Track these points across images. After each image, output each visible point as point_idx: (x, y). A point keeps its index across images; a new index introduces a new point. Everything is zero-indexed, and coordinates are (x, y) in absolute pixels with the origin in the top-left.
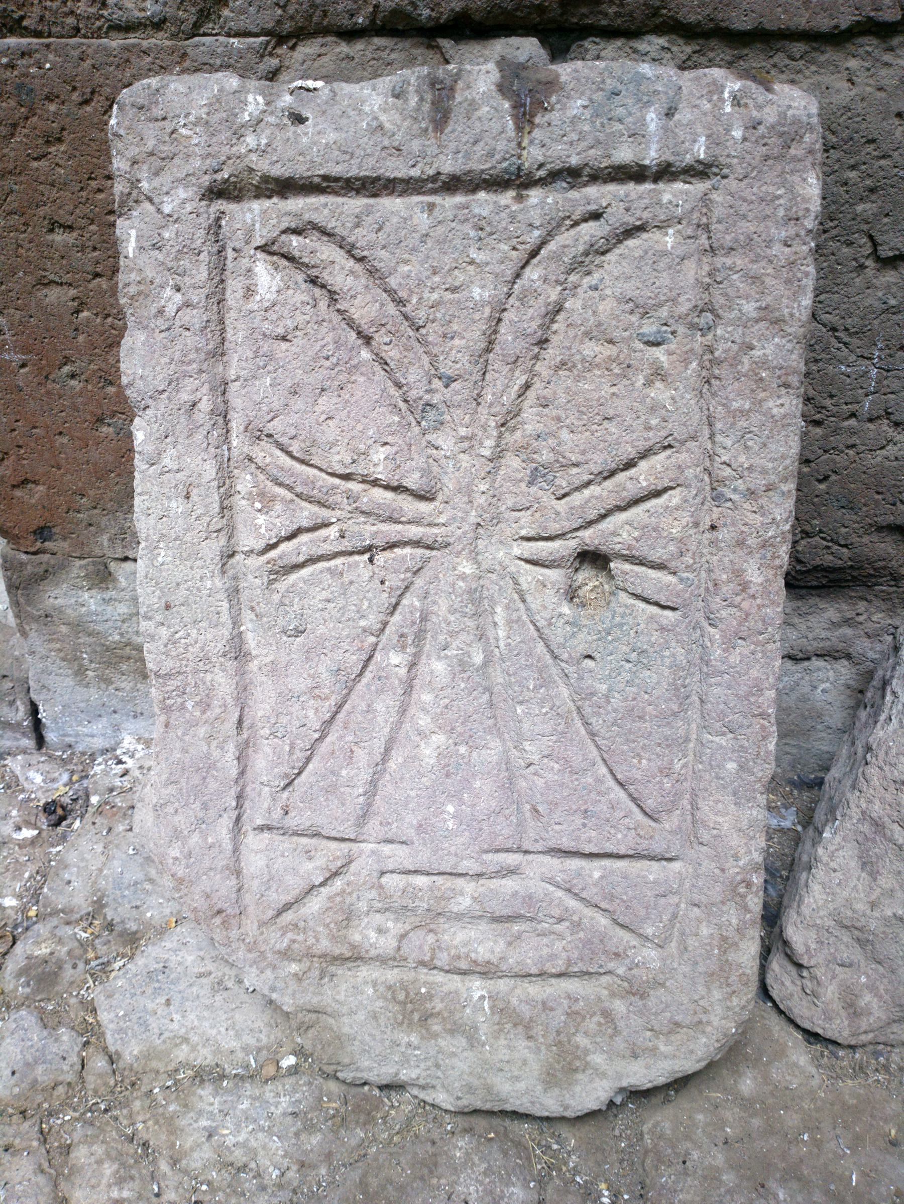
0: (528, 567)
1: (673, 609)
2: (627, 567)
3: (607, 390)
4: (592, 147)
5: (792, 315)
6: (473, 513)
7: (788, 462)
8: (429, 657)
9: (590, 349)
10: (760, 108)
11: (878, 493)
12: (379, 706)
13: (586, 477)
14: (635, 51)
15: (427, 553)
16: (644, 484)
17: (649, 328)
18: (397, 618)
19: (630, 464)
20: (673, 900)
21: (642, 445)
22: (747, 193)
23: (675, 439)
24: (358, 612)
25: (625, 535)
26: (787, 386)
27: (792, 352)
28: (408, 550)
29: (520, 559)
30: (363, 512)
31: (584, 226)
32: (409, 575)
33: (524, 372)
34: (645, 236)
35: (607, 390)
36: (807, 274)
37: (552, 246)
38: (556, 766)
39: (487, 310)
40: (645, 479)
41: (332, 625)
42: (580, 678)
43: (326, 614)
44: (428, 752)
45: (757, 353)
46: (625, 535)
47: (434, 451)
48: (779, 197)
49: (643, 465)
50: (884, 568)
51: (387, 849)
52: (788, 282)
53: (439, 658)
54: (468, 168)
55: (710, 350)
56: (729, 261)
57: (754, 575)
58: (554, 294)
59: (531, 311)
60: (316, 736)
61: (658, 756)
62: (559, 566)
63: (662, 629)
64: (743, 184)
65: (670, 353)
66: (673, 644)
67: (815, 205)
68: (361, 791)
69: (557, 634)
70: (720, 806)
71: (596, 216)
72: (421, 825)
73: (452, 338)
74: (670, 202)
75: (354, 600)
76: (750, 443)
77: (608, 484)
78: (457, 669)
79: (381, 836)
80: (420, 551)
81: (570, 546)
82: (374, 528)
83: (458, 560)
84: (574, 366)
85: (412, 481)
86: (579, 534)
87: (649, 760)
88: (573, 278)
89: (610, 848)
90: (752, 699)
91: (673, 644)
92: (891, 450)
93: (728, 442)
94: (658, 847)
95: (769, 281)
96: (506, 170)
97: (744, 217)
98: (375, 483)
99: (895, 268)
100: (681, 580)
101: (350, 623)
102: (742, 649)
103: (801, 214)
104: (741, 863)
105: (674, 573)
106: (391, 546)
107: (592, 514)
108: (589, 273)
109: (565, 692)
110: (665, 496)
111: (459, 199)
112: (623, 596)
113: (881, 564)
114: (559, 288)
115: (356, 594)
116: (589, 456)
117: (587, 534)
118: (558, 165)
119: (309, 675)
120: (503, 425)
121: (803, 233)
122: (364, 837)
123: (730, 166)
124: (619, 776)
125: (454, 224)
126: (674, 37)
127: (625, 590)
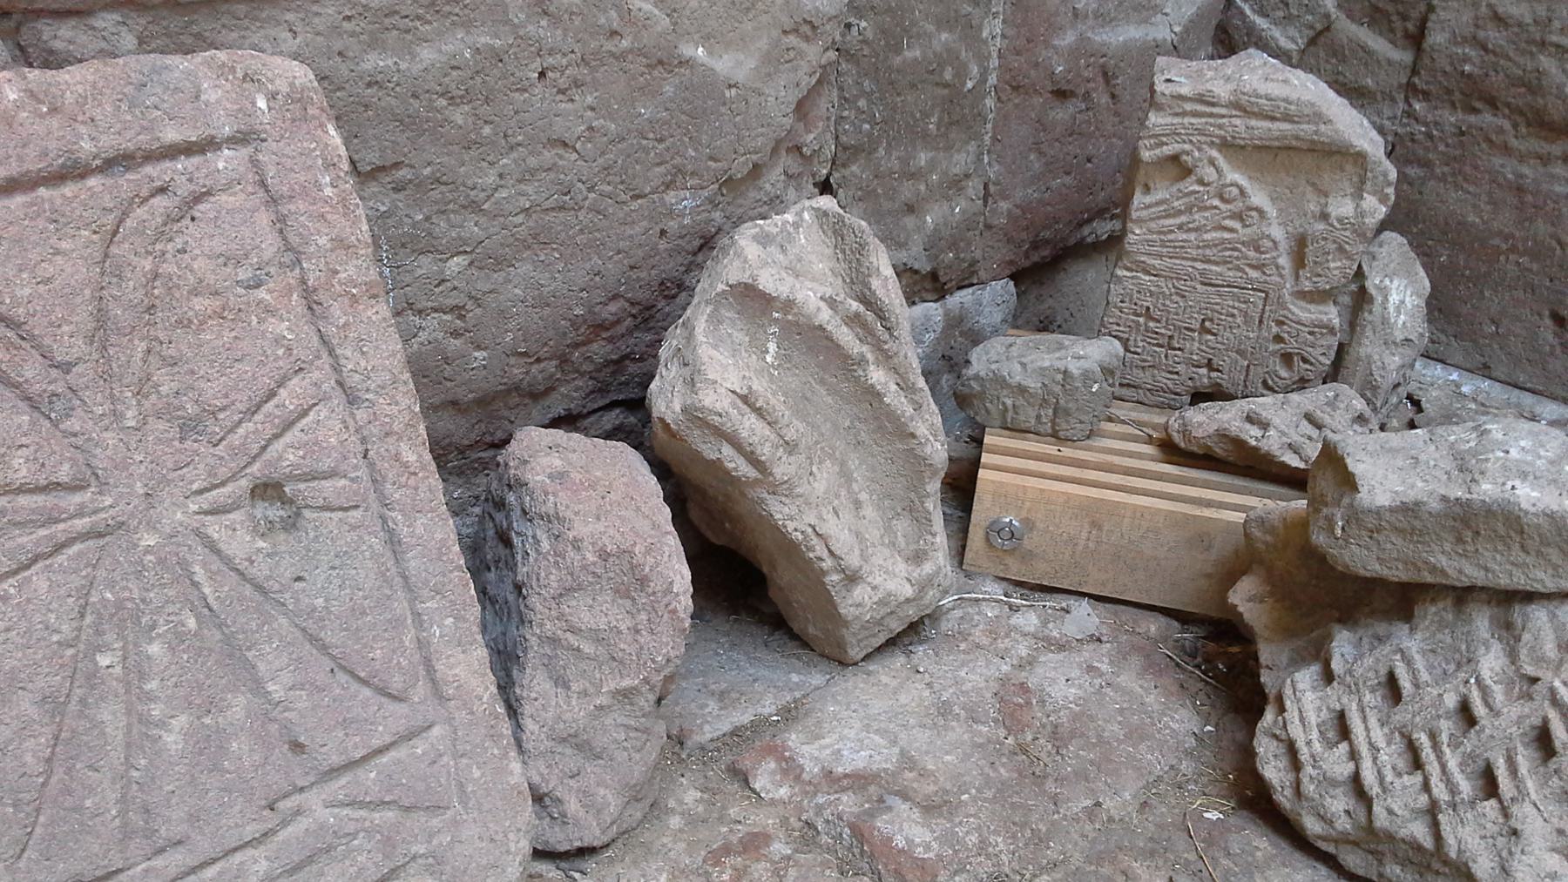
0: (209, 518)
1: (357, 507)
2: (302, 486)
3: (227, 336)
4: (139, 134)
5: (358, 240)
6: (139, 484)
7: (399, 356)
8: (136, 645)
9: (200, 304)
10: (272, 81)
11: (424, 377)
12: (106, 716)
13: (236, 418)
14: (93, 28)
15: (102, 542)
16: (292, 407)
17: (243, 275)
18: (89, 619)
19: (272, 394)
20: (445, 759)
21: (277, 375)
22: (287, 151)
23: (304, 362)
24: (47, 628)
25: (291, 457)
26: (374, 296)
27: (368, 268)
28: (76, 548)
29: (198, 513)
30: (16, 524)
31: (152, 201)
32: (89, 570)
33: (142, 339)
34: (212, 199)
35: (227, 336)
36: (357, 205)
37: (129, 223)
38: (303, 693)
39: (87, 292)
40: (291, 403)
41: (20, 655)
42: (298, 600)
43: (10, 646)
44: (172, 740)
45: (343, 275)
46: (291, 457)
47: (73, 439)
48: (315, 149)
49: (283, 393)
50: (450, 444)
51: (158, 862)
52: (345, 215)
53: (151, 640)
54: (25, 169)
55: (303, 282)
56: (293, 207)
57: (410, 457)
58: (147, 264)
59: (131, 283)
60: (41, 780)
61: (388, 640)
62: (238, 507)
63: (354, 528)
64: (281, 144)
65: (270, 291)
66: (367, 538)
67: (343, 151)
68: (114, 812)
69: (260, 570)
70: (452, 660)
71: (162, 190)
72: (191, 815)
73: (59, 326)
74: (226, 168)
75: (37, 618)
76: (365, 349)
77: (258, 417)
78: (174, 643)
79: (149, 851)
80: (91, 543)
81: (244, 483)
82: (34, 536)
83: (139, 536)
84: (190, 321)
85: (64, 474)
86: (248, 471)
87: (382, 648)
88: (158, 247)
89: (376, 743)
90: (445, 558)
91: (367, 538)
92: (423, 336)
93: (349, 353)
94: (419, 721)
95: (329, 217)
96: (63, 166)
97: (292, 170)
98: (21, 490)
99: (374, 179)
100: (352, 480)
101: (43, 643)
102: (422, 520)
103: (336, 160)
104: (485, 700)
105: (345, 476)
106: (59, 548)
107: (255, 448)
108: (171, 240)
109: (283, 620)
110: (312, 413)
111: (19, 199)
112: (307, 513)
113: (447, 441)
114: (151, 258)
115: (38, 611)
116: (233, 396)
117: (255, 468)
118: (111, 154)
119: (11, 718)
120: (138, 394)
121: (342, 174)
122: (132, 861)
123: (266, 132)
124: (362, 675)
125: (26, 222)
126: (126, 11)
127: (307, 506)
